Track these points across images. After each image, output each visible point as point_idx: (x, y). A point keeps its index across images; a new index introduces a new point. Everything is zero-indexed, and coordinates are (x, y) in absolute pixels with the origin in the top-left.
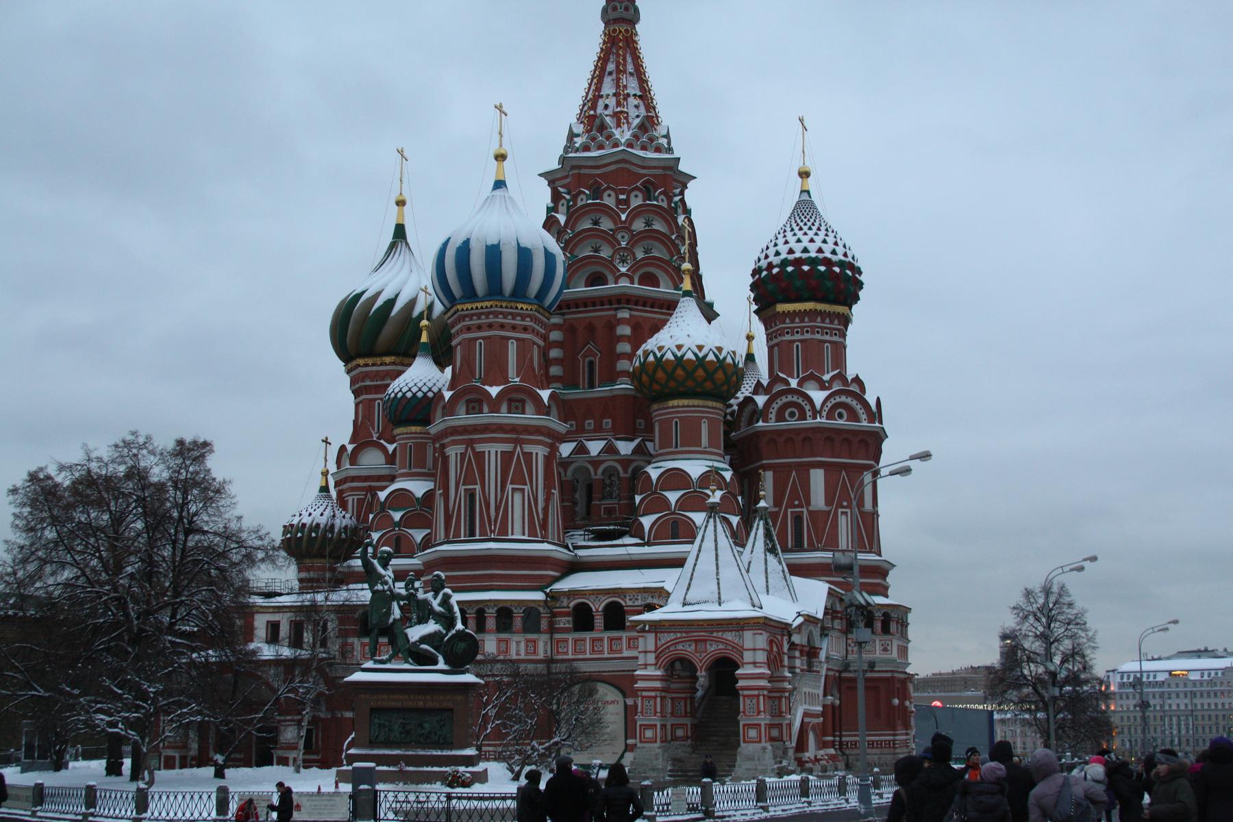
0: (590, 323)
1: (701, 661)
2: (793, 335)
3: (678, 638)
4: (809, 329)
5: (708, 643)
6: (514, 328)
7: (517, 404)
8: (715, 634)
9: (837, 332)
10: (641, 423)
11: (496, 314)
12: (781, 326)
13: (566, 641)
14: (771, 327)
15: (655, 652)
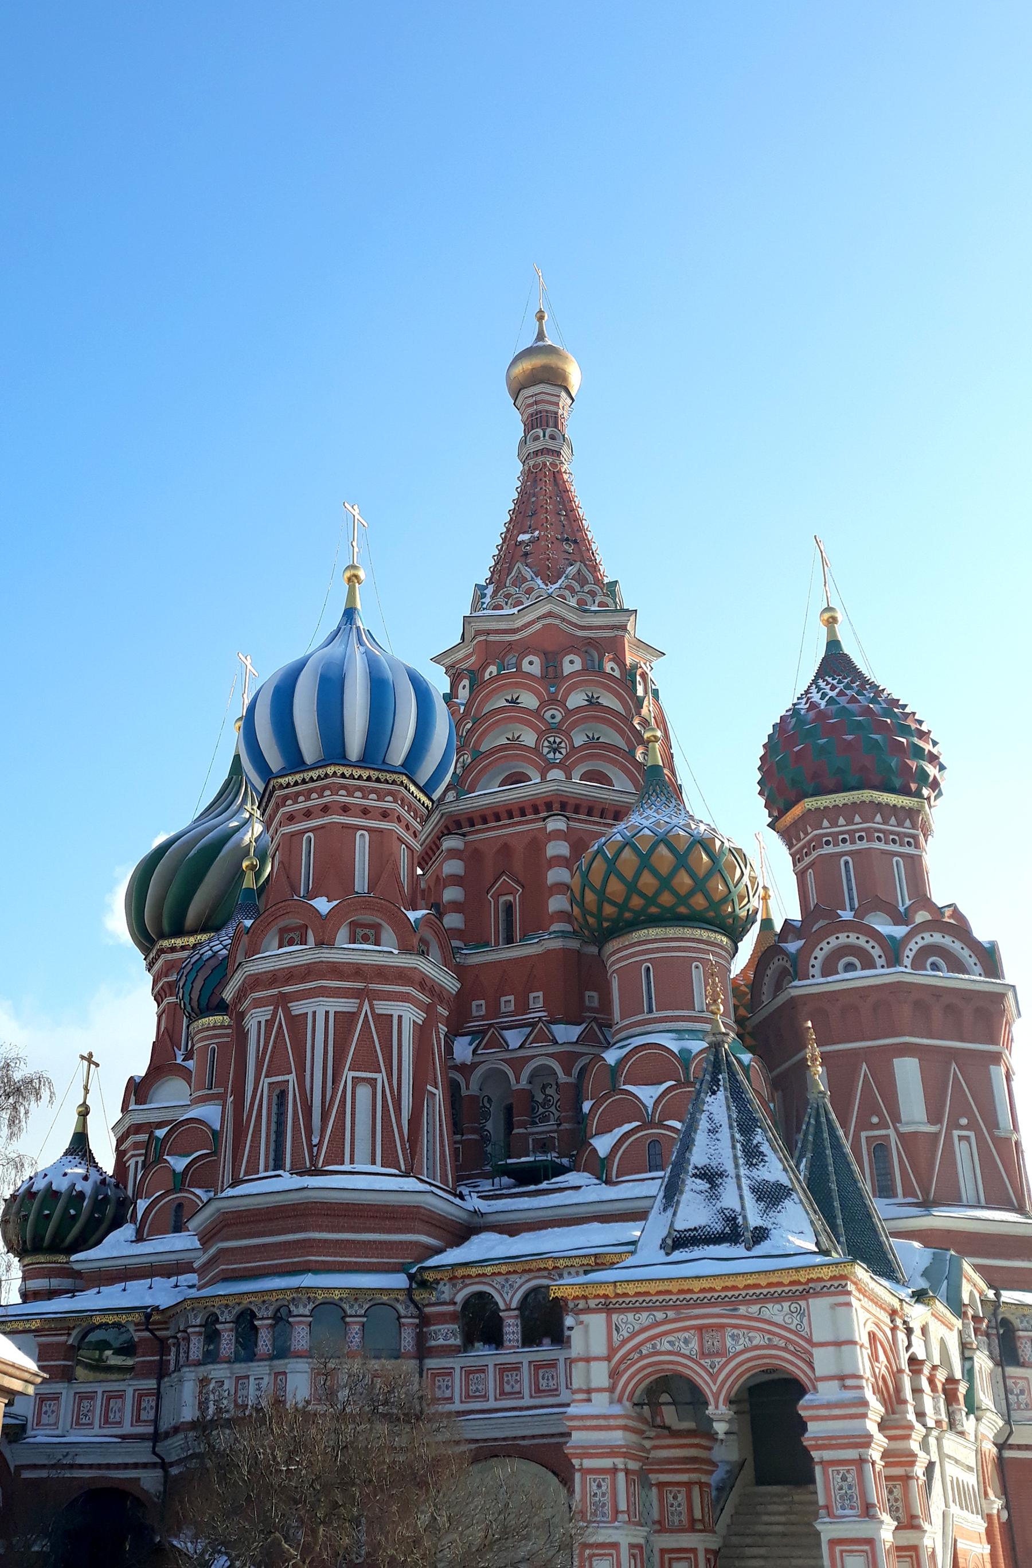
0: (506, 844)
1: (714, 1377)
2: (836, 845)
3: (657, 1324)
4: (863, 834)
5: (730, 1331)
6: (365, 812)
7: (366, 931)
8: (742, 1310)
9: (911, 840)
10: (592, 997)
11: (335, 789)
12: (816, 832)
13: (448, 1373)
14: (799, 840)
15: (608, 1359)
